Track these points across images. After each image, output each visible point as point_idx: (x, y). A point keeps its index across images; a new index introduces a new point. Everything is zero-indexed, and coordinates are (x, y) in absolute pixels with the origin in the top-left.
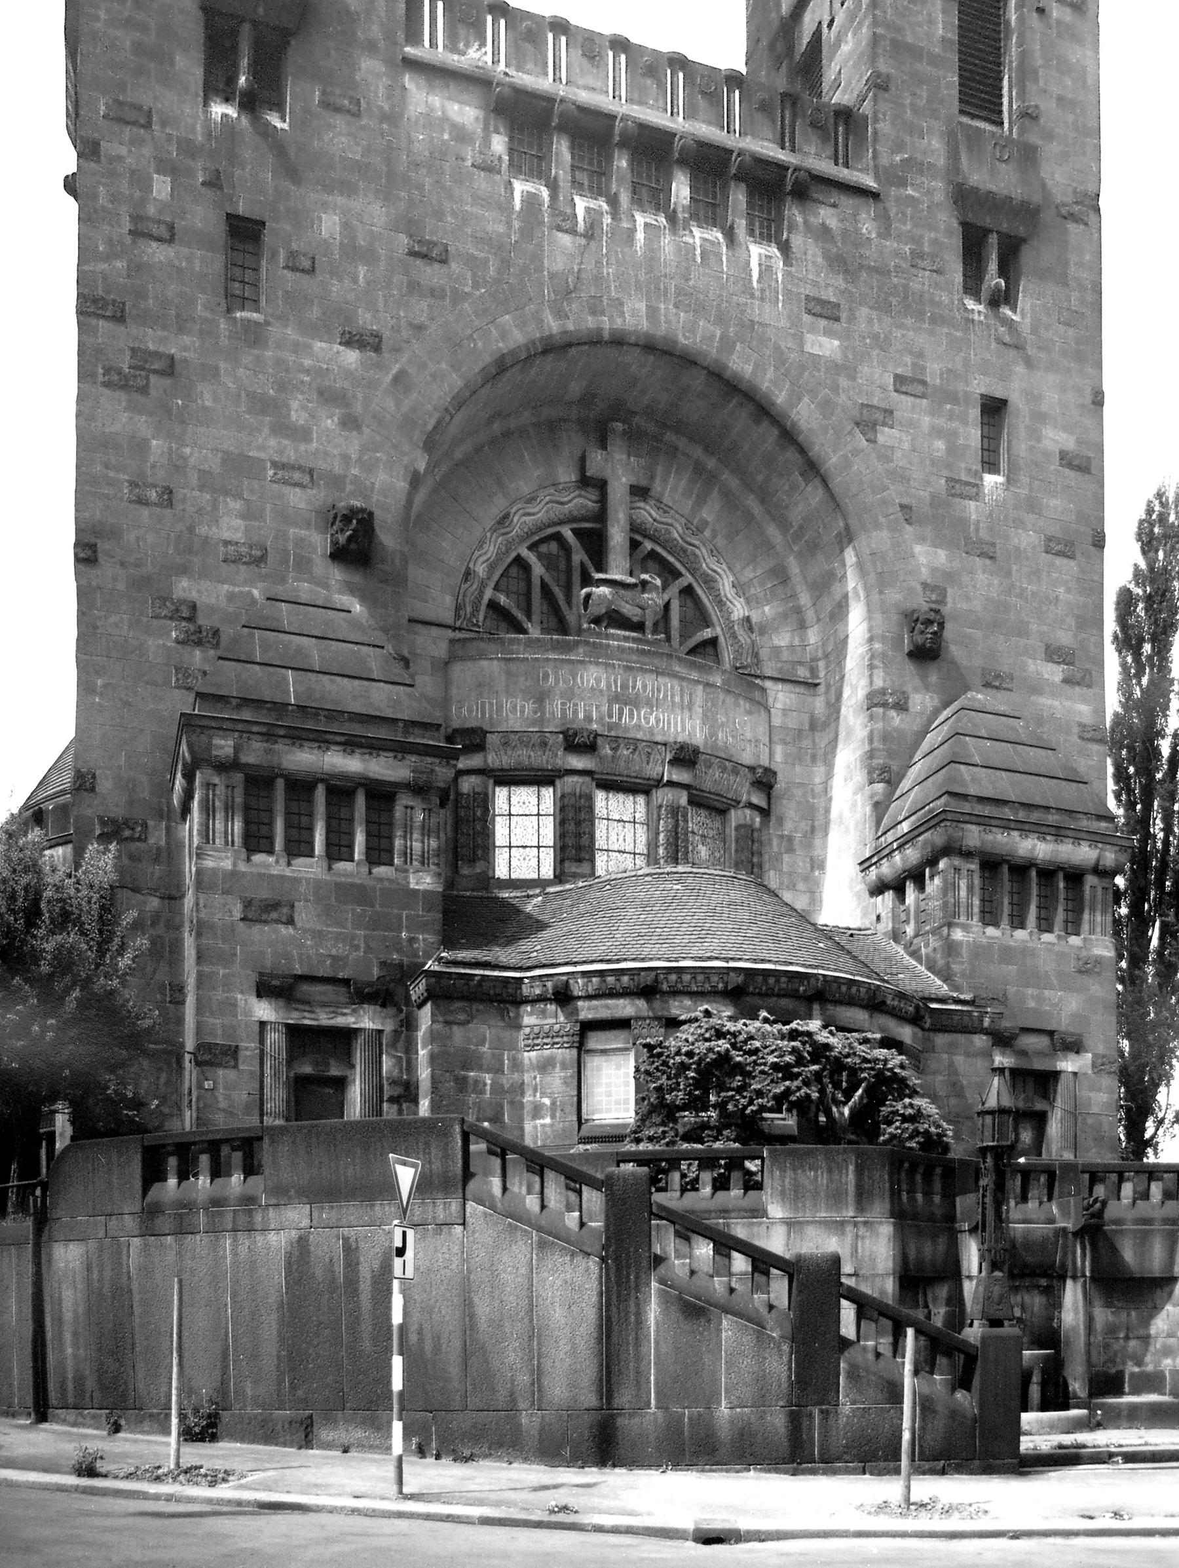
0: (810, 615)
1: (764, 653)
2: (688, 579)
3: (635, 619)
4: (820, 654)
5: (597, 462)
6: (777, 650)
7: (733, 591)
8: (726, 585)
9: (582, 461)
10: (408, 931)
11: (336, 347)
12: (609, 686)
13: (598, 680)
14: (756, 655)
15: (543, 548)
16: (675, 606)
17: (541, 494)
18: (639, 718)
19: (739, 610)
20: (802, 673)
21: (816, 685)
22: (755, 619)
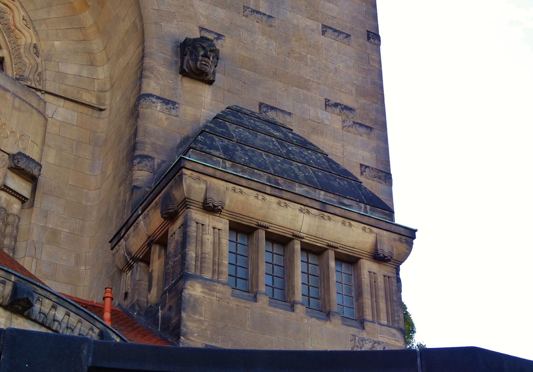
0: (100, 56)
1: (48, 75)
4: (108, 86)
6: (61, 76)
7: (23, 23)
14: (40, 74)
19: (27, 37)
20: (87, 98)
21: (101, 110)
22: (43, 47)
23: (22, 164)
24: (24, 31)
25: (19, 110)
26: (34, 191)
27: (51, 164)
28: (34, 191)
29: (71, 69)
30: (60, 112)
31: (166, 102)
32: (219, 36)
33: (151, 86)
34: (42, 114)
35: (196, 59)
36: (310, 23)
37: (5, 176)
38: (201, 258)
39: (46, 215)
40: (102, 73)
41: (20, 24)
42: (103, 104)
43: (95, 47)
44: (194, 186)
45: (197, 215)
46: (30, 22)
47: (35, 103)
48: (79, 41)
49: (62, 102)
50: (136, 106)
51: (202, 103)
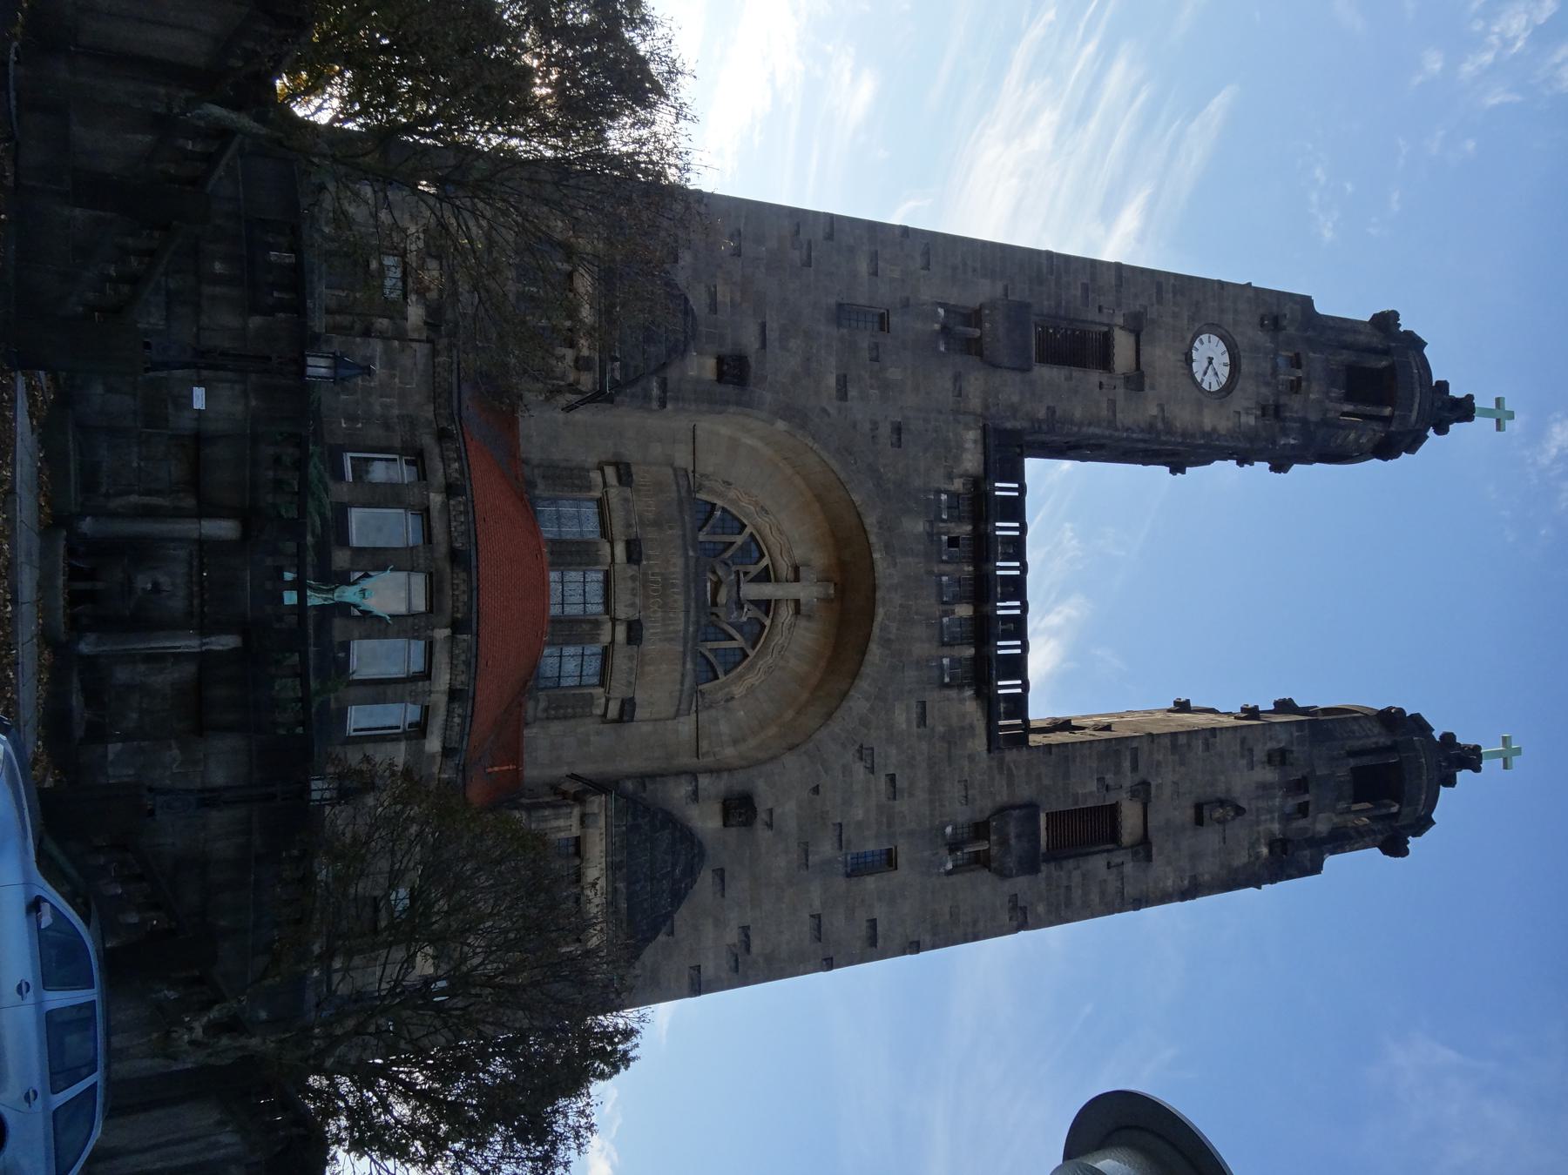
1: (713, 712)
2: (752, 654)
8: (752, 679)
13: (675, 565)
14: (710, 707)
15: (753, 546)
16: (733, 644)
19: (738, 691)
20: (704, 745)
23: (627, 707)
26: (613, 721)
27: (640, 729)
28: (613, 721)
30: (686, 726)
31: (695, 792)
32: (770, 825)
33: (704, 781)
34: (677, 714)
35: (739, 809)
36: (817, 903)
38: (545, 819)
39: (598, 733)
40: (729, 752)
44: (596, 804)
45: (576, 811)
46: (751, 690)
47: (684, 706)
50: (686, 773)
51: (706, 821)
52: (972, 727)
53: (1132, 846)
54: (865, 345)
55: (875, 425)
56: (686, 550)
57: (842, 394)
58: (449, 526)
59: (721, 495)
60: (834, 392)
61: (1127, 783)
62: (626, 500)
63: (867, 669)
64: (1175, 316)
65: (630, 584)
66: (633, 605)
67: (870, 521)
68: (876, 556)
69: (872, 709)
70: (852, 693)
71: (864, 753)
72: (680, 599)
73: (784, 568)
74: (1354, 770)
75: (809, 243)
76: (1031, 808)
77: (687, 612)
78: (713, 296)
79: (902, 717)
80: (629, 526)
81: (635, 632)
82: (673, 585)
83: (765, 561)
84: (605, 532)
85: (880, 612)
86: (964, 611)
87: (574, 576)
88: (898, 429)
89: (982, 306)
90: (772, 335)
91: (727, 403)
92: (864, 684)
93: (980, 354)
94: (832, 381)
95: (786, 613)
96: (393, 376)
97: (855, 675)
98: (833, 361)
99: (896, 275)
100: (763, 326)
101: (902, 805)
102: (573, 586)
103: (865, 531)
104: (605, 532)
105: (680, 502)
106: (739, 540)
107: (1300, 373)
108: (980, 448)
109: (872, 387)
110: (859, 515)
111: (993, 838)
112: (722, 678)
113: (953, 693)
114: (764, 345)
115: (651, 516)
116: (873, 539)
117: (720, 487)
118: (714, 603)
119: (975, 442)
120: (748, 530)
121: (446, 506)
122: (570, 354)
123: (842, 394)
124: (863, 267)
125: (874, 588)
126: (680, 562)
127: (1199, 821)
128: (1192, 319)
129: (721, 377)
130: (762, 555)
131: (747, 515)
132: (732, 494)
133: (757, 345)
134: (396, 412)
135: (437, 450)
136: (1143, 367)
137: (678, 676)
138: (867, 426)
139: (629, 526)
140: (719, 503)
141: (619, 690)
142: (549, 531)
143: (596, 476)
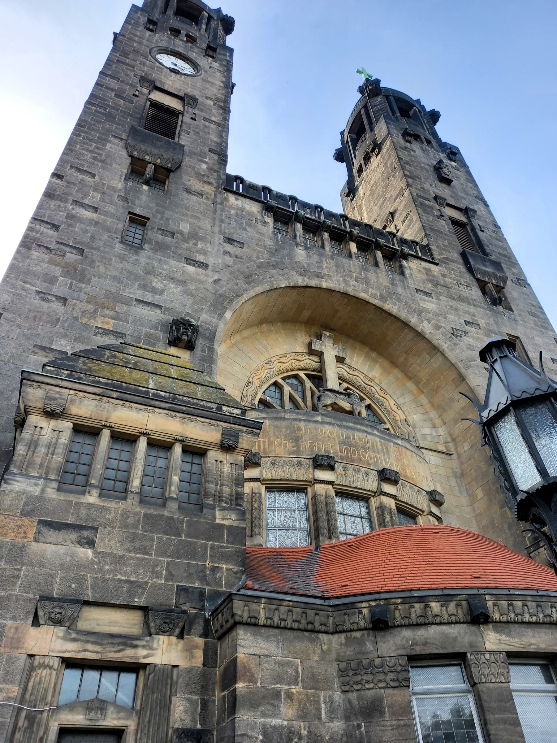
2: (368, 402)
3: (347, 409)
5: (316, 346)
6: (424, 436)
9: (310, 345)
10: (212, 561)
11: (183, 264)
12: (339, 437)
13: (331, 433)
17: (289, 355)
18: (359, 455)
19: (400, 416)
20: (441, 448)
21: (450, 455)
22: (410, 419)
24: (397, 412)
25: (420, 462)
29: (427, 431)
37: (429, 506)
41: (394, 408)
42: (450, 451)
43: (432, 416)
48: (424, 414)
49: (430, 453)
52: (425, 269)
53: (468, 218)
54: (160, 237)
55: (226, 253)
56: (316, 422)
57: (204, 266)
58: (530, 623)
59: (257, 390)
60: (200, 270)
61: (438, 207)
62: (274, 463)
63: (403, 315)
64: (144, 64)
65: (350, 472)
66: (367, 474)
67: (301, 281)
68: (324, 285)
69: (429, 320)
70: (419, 330)
71: (455, 334)
72: (357, 434)
73: (311, 362)
74: (402, 116)
75: (58, 242)
76: (464, 255)
77: (366, 432)
78: (107, 332)
79: (430, 305)
80: (299, 464)
81: (385, 476)
82: (348, 437)
83: (302, 374)
84: (298, 488)
85: (363, 295)
86: (353, 247)
87: (341, 523)
88: (230, 241)
89: (132, 157)
90: (149, 297)
91: (211, 349)
92: (413, 320)
93: (169, 171)
94: (191, 269)
95: (344, 370)
96: (289, 696)
97: (406, 325)
98: (173, 262)
99: (99, 196)
100: (139, 301)
101: (482, 322)
102: (348, 525)
103: (306, 287)
104: (298, 488)
105: (277, 419)
106: (287, 389)
107: (183, 33)
108: (240, 198)
109: (196, 245)
110: (294, 287)
111: (486, 279)
112: (388, 426)
113: (407, 272)
114: (160, 307)
115: (290, 444)
116: (313, 283)
117: (251, 391)
118: (351, 413)
119: (237, 199)
120: (280, 381)
121: (503, 625)
122: (213, 455)
123: (204, 266)
124: (88, 214)
125: (345, 295)
126: (328, 428)
127: (448, 182)
128: (146, 57)
129: (190, 346)
130: (296, 377)
131: (271, 377)
132: (256, 382)
133: (158, 311)
134: (337, 696)
135: (407, 633)
136: (181, 94)
137: (408, 452)
138: (227, 258)
139: (299, 464)
140: (260, 395)
141: (423, 503)
142: (299, 539)
143: (247, 488)
